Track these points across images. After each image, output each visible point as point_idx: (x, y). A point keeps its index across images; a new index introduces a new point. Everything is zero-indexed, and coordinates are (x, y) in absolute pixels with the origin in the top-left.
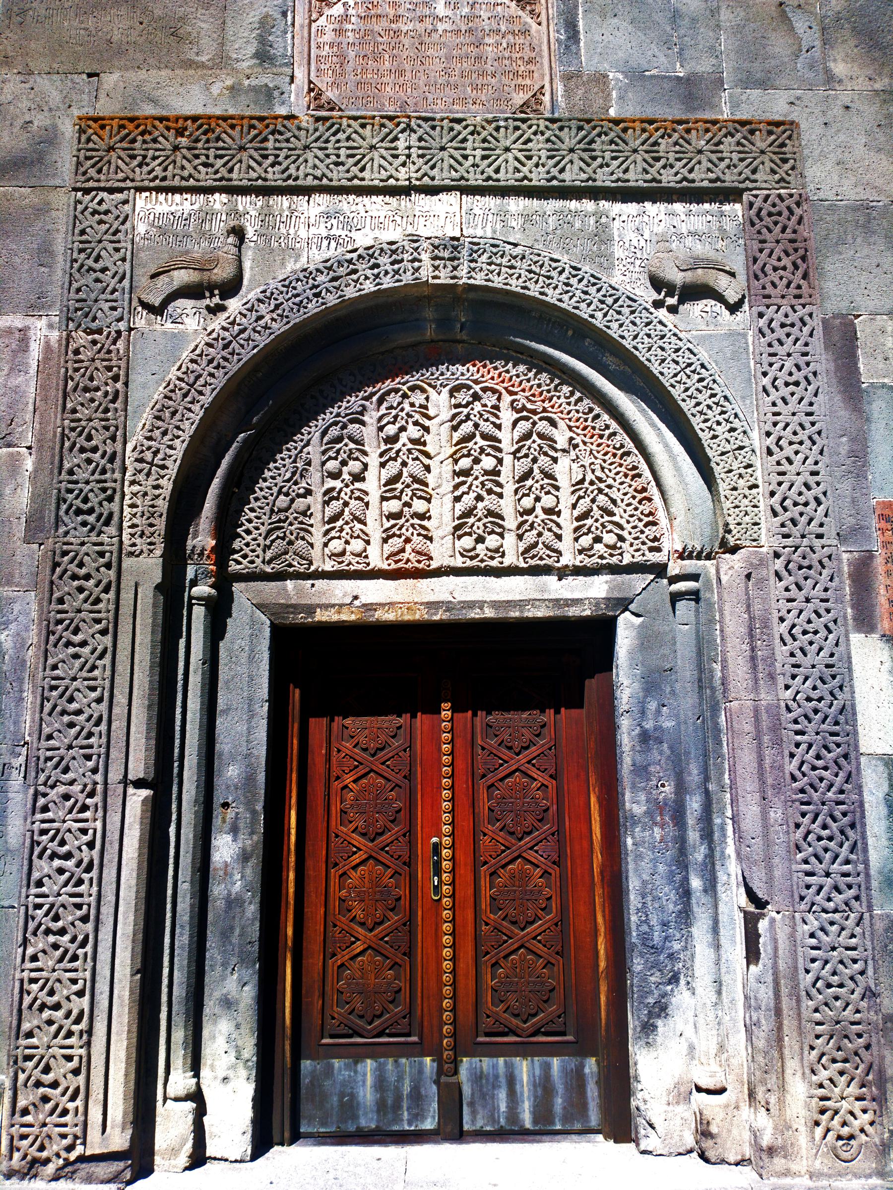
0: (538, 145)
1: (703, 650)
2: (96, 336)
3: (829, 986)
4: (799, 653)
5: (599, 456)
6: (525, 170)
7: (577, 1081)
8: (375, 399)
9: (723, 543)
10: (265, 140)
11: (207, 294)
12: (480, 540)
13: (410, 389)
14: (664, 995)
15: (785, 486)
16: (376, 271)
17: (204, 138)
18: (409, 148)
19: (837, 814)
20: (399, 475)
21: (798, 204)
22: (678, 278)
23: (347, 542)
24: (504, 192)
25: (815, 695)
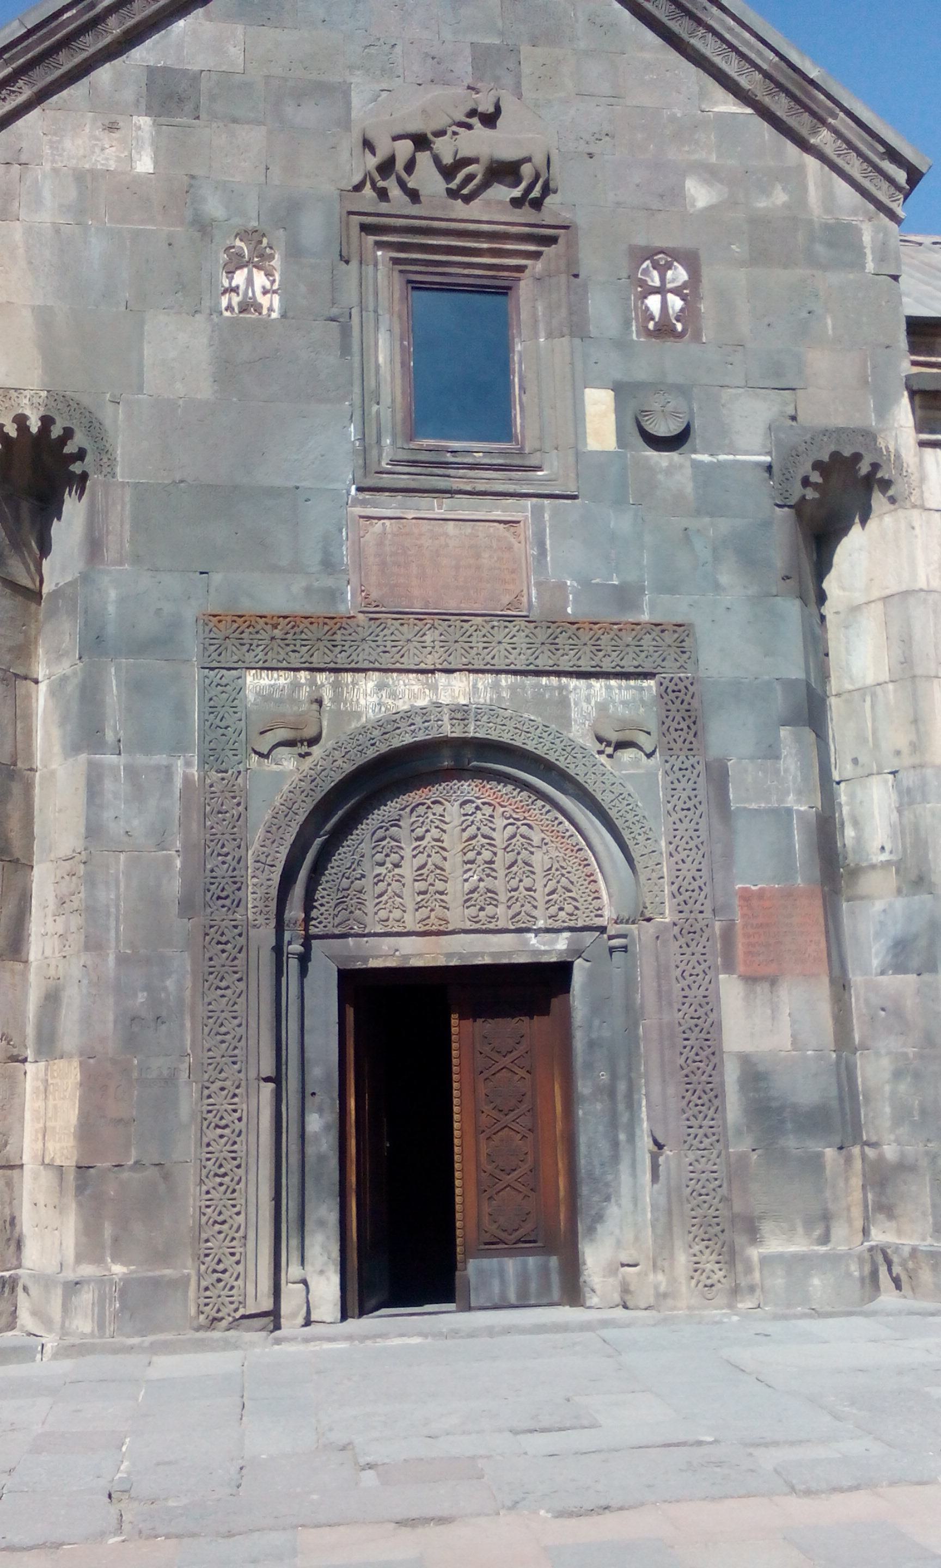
0: (520, 639)
1: (630, 985)
2: (224, 774)
3: (700, 1195)
4: (686, 988)
5: (562, 850)
6: (512, 657)
7: (545, 1272)
8: (408, 810)
9: (642, 914)
10: (335, 633)
11: (299, 744)
12: (482, 909)
13: (433, 803)
14: (602, 1209)
15: (681, 878)
16: (413, 727)
17: (292, 631)
18: (433, 642)
19: (708, 1090)
20: (426, 864)
21: (692, 684)
22: (614, 737)
23: (390, 912)
24: (498, 672)
25: (696, 1015)
